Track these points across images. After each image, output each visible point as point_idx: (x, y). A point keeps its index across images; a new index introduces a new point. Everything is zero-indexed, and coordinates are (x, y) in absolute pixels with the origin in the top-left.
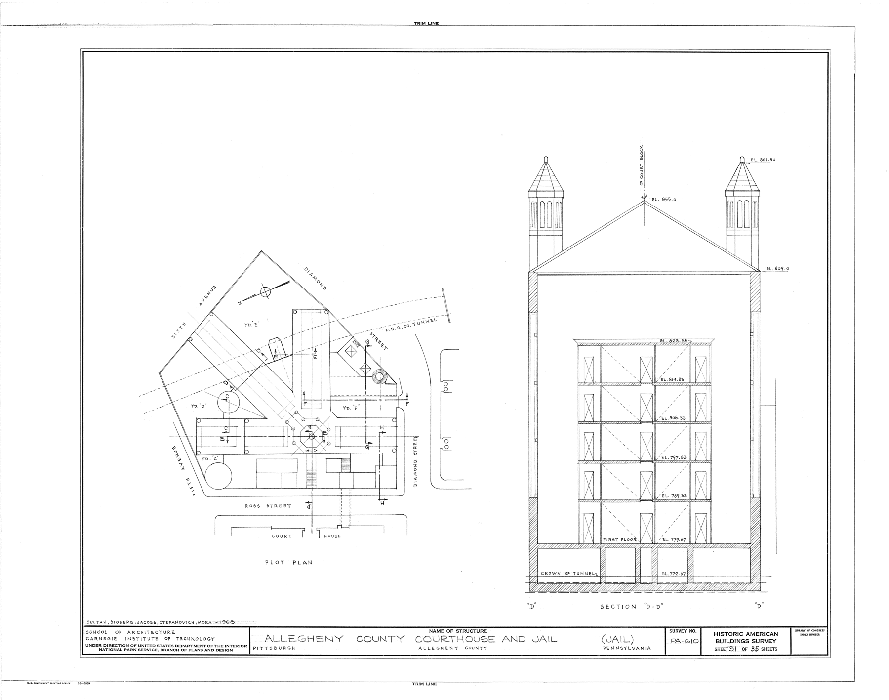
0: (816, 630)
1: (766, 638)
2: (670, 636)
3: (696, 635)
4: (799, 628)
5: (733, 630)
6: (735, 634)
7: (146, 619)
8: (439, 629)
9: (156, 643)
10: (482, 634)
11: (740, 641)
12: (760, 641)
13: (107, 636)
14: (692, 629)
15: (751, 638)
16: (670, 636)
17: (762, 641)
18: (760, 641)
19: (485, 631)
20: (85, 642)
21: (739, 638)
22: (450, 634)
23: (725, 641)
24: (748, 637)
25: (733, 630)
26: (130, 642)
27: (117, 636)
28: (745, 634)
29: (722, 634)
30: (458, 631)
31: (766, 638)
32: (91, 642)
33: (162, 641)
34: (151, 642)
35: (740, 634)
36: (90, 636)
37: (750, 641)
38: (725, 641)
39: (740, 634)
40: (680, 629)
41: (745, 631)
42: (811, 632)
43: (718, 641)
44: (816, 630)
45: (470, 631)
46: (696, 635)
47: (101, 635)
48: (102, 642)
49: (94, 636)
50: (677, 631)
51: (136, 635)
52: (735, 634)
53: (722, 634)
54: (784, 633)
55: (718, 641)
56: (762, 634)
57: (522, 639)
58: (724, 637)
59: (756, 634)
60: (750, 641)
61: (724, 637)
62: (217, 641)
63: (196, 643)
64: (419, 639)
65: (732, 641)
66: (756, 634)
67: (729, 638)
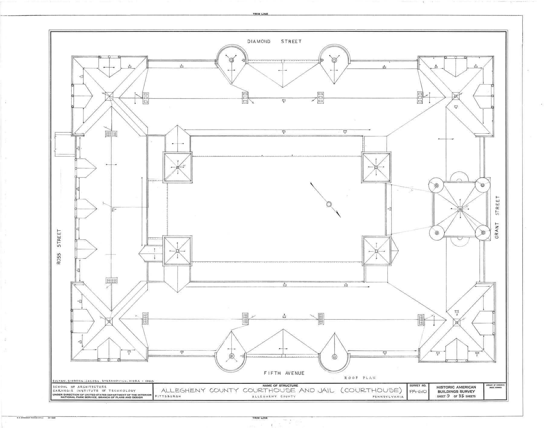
0: (499, 385)
1: (469, 389)
2: (410, 388)
3: (426, 388)
4: (489, 384)
5: (448, 385)
6: (449, 387)
7: (92, 379)
8: (269, 384)
9: (96, 393)
10: (295, 387)
11: (453, 392)
12: (464, 391)
13: (66, 389)
14: (424, 384)
15: (459, 390)
16: (410, 388)
17: (466, 391)
18: (464, 391)
19: (297, 386)
20: (53, 393)
21: (452, 389)
22: (275, 387)
23: (444, 392)
24: (457, 389)
25: (448, 385)
26: (80, 393)
27: (73, 389)
28: (456, 387)
29: (442, 387)
30: (280, 386)
31: (469, 389)
32: (56, 393)
33: (100, 392)
34: (93, 393)
35: (452, 387)
36: (55, 389)
37: (459, 391)
38: (444, 392)
39: (452, 387)
40: (416, 384)
41: (456, 385)
42: (496, 386)
43: (439, 392)
44: (499, 385)
45: (287, 386)
46: (426, 388)
47: (63, 389)
48: (63, 393)
49: (58, 389)
50: (414, 385)
51: (60, 389)
52: (449, 387)
53: (442, 387)
54: (480, 387)
55: (439, 392)
56: (466, 387)
57: (312, 390)
58: (443, 389)
59: (463, 387)
60: (459, 391)
61: (443, 389)
62: (137, 393)
63: (119, 393)
64: (245, 390)
65: (449, 392)
66: (463, 387)
67: (446, 390)
